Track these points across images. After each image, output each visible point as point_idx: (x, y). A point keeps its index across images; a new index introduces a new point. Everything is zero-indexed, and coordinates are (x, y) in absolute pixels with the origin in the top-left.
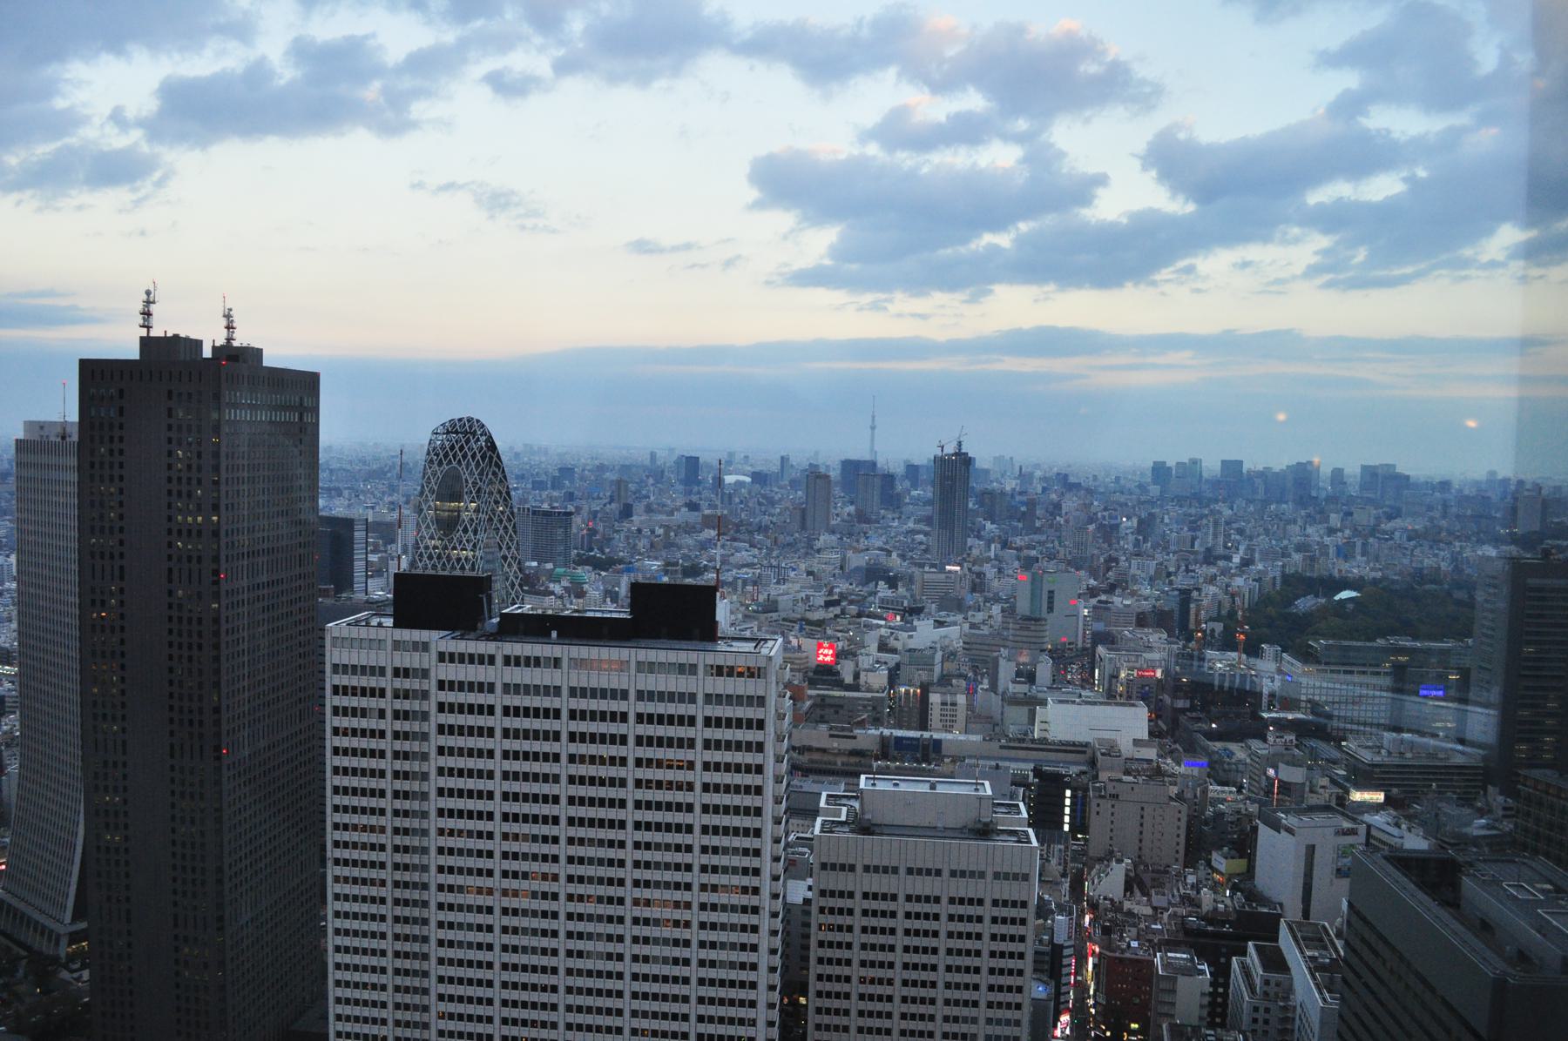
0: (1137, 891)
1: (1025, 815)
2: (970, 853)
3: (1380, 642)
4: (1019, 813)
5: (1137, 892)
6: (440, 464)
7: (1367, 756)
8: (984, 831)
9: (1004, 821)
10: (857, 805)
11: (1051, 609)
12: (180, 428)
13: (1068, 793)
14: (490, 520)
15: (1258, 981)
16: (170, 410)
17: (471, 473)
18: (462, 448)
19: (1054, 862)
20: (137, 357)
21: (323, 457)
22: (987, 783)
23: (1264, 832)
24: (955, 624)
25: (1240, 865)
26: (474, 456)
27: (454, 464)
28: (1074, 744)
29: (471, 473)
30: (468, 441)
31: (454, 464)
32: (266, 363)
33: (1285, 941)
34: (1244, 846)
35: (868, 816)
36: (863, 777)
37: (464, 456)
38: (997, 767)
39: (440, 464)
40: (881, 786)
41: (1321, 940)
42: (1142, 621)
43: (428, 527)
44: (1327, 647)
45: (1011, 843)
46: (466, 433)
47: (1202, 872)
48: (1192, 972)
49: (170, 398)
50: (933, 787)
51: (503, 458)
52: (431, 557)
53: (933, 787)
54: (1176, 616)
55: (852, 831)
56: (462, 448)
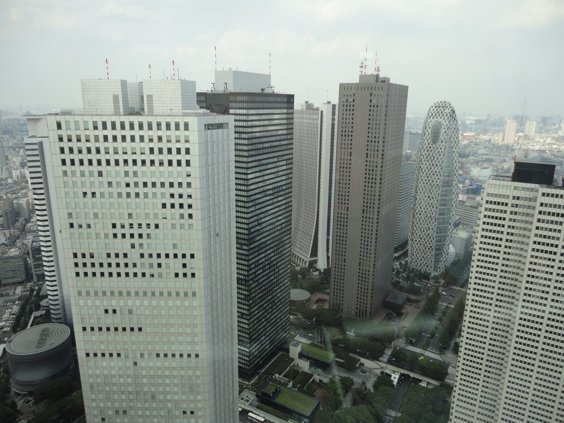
6: (433, 118)
12: (374, 106)
14: (450, 138)
16: (371, 100)
17: (445, 121)
18: (442, 112)
20: (357, 81)
21: (408, 116)
26: (447, 115)
27: (439, 118)
29: (445, 121)
30: (444, 110)
31: (439, 118)
32: (391, 82)
37: (443, 115)
39: (433, 118)
43: (428, 140)
46: (443, 107)
49: (371, 96)
51: (457, 116)
52: (428, 151)
56: (442, 112)
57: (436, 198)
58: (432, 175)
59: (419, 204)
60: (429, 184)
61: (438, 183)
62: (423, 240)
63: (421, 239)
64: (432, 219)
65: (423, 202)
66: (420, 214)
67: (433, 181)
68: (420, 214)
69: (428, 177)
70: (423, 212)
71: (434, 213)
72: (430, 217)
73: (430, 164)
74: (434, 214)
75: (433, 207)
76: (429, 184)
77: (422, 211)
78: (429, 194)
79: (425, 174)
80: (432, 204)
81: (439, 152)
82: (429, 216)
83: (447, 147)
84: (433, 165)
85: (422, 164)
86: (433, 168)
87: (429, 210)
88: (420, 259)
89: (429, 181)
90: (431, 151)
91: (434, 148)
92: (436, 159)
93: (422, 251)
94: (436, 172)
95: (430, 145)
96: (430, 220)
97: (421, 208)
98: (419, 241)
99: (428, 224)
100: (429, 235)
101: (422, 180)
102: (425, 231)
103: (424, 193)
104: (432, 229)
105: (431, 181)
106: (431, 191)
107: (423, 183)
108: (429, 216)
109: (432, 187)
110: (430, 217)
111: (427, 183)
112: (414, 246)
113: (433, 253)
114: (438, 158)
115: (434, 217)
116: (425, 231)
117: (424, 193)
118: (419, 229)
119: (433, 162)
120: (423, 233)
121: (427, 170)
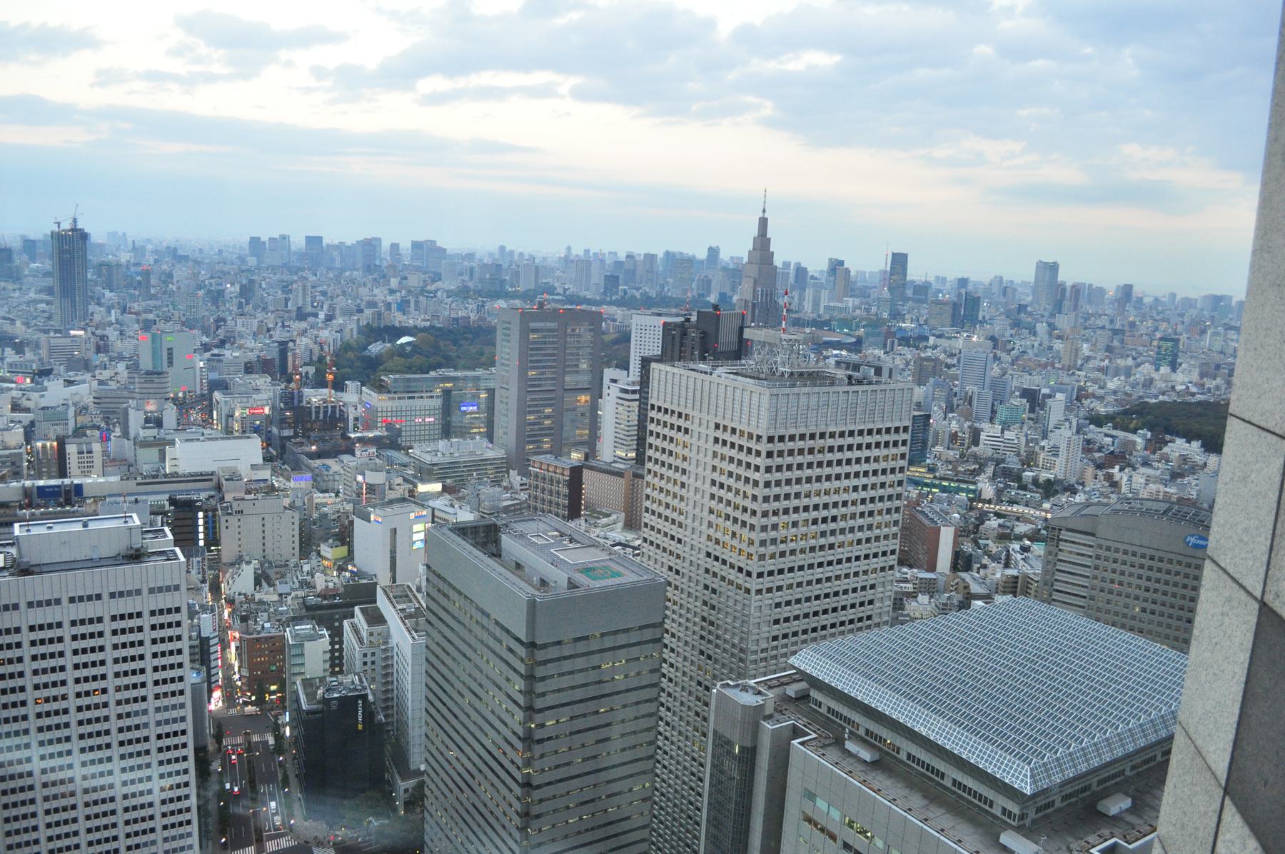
0: (264, 584)
1: (170, 537)
2: (127, 576)
3: (432, 374)
4: (165, 536)
5: (264, 584)
7: (428, 459)
8: (136, 556)
9: (153, 545)
10: (13, 551)
11: (170, 363)
13: (201, 515)
15: (364, 635)
19: (193, 572)
22: (134, 515)
23: (358, 522)
24: (84, 382)
25: (342, 551)
28: (201, 475)
33: (382, 603)
34: (344, 537)
35: (25, 560)
36: (16, 525)
38: (136, 501)
40: (37, 530)
41: (407, 596)
42: (249, 369)
44: (396, 380)
45: (161, 562)
47: (314, 562)
48: (312, 638)
50: (85, 525)
53: (85, 525)
54: (277, 363)
55: (12, 575)
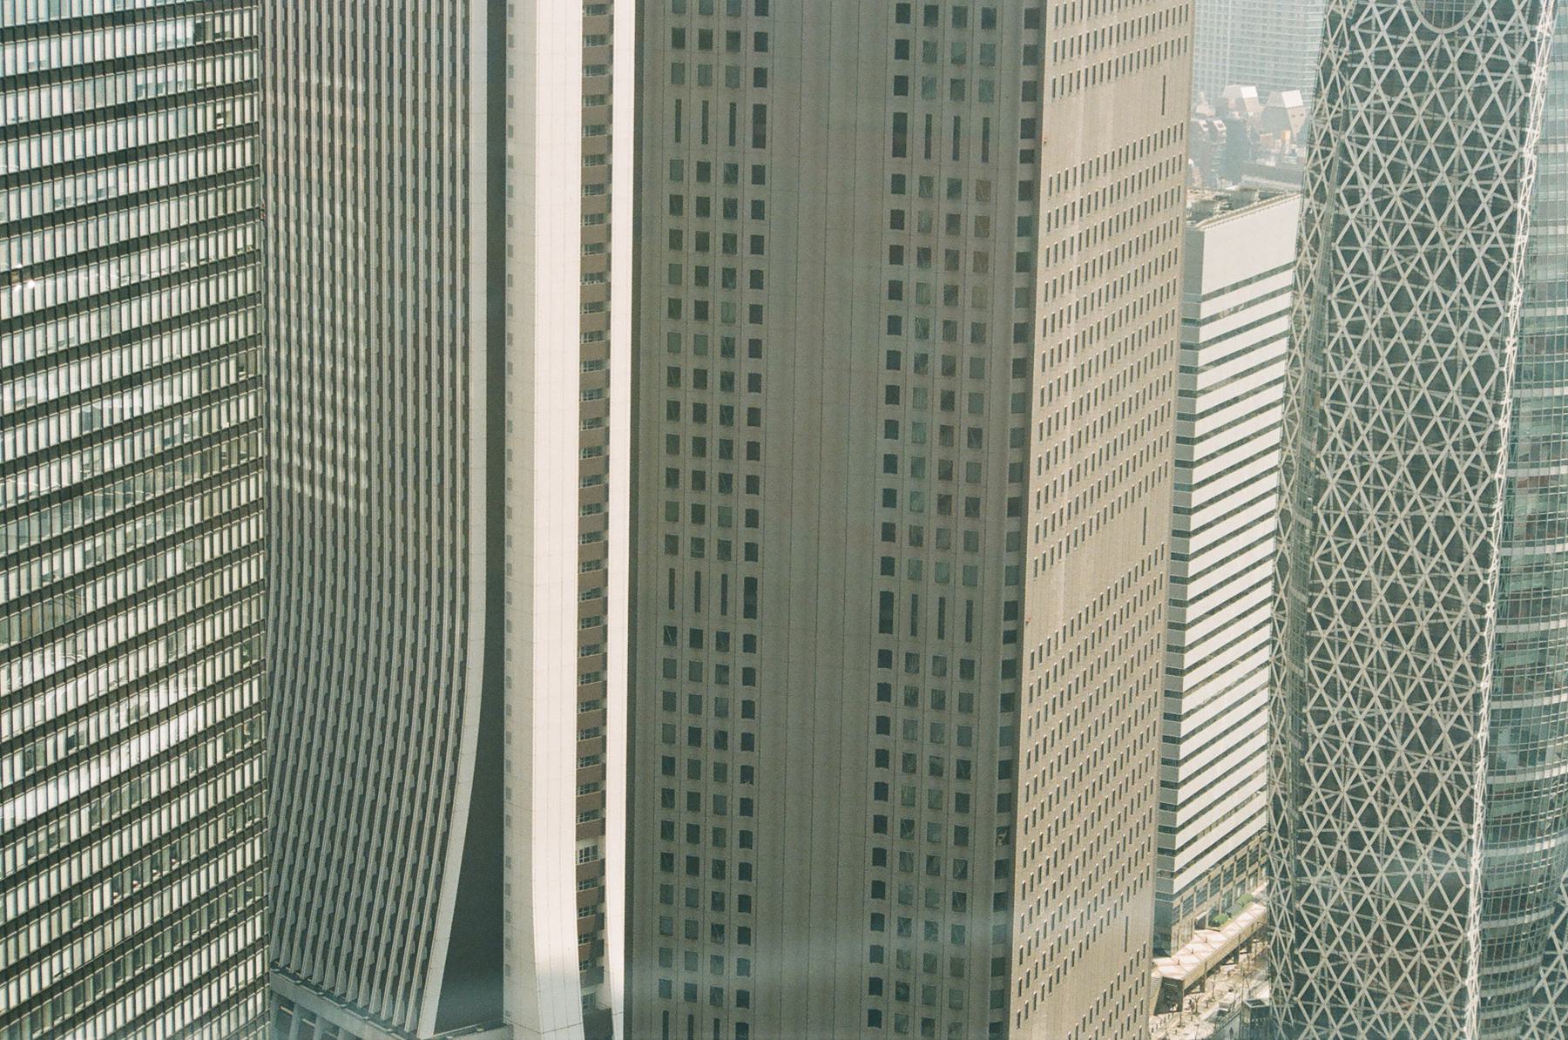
52: (1392, 86)
57: (1473, 476)
58: (1433, 286)
59: (1343, 531)
60: (1413, 361)
61: (1485, 348)
62: (1383, 828)
63: (1370, 820)
64: (1447, 651)
65: (1371, 511)
66: (1353, 616)
67: (1443, 336)
68: (1353, 616)
69: (1401, 303)
70: (1379, 598)
71: (1467, 598)
72: (1437, 630)
73: (1412, 197)
74: (1466, 613)
75: (1455, 553)
76: (1413, 361)
77: (1365, 590)
78: (1420, 447)
79: (1375, 273)
80: (1444, 524)
81: (1480, 94)
82: (1422, 627)
83: (1542, 53)
84: (1440, 197)
85: (1353, 198)
86: (1438, 225)
87: (1425, 577)
88: (1364, 987)
89: (1413, 332)
90: (1420, 84)
91: (1443, 60)
92: (1459, 149)
93: (1380, 920)
94: (1467, 257)
95: (1411, 39)
96: (1433, 656)
97: (1356, 562)
98: (1356, 841)
99: (1417, 696)
100: (1428, 781)
101: (1356, 328)
102: (1400, 749)
103: (1379, 440)
104: (1458, 736)
105: (1427, 338)
106: (1437, 417)
107: (1370, 356)
108: (1422, 627)
109: (1440, 385)
110: (1437, 630)
111: (1396, 355)
112: (1314, 882)
113: (1472, 933)
114: (1474, 139)
115: (1465, 631)
116: (1400, 749)
117: (1379, 440)
118: (1346, 741)
119: (1441, 178)
120: (1386, 772)
121: (1391, 248)
